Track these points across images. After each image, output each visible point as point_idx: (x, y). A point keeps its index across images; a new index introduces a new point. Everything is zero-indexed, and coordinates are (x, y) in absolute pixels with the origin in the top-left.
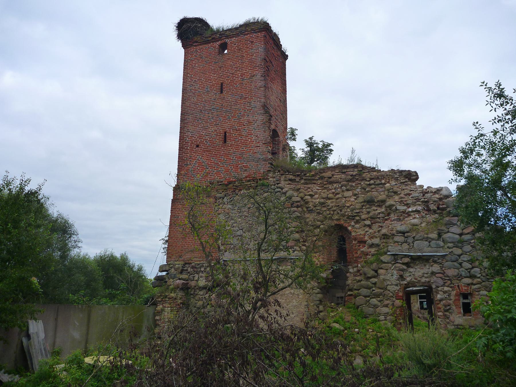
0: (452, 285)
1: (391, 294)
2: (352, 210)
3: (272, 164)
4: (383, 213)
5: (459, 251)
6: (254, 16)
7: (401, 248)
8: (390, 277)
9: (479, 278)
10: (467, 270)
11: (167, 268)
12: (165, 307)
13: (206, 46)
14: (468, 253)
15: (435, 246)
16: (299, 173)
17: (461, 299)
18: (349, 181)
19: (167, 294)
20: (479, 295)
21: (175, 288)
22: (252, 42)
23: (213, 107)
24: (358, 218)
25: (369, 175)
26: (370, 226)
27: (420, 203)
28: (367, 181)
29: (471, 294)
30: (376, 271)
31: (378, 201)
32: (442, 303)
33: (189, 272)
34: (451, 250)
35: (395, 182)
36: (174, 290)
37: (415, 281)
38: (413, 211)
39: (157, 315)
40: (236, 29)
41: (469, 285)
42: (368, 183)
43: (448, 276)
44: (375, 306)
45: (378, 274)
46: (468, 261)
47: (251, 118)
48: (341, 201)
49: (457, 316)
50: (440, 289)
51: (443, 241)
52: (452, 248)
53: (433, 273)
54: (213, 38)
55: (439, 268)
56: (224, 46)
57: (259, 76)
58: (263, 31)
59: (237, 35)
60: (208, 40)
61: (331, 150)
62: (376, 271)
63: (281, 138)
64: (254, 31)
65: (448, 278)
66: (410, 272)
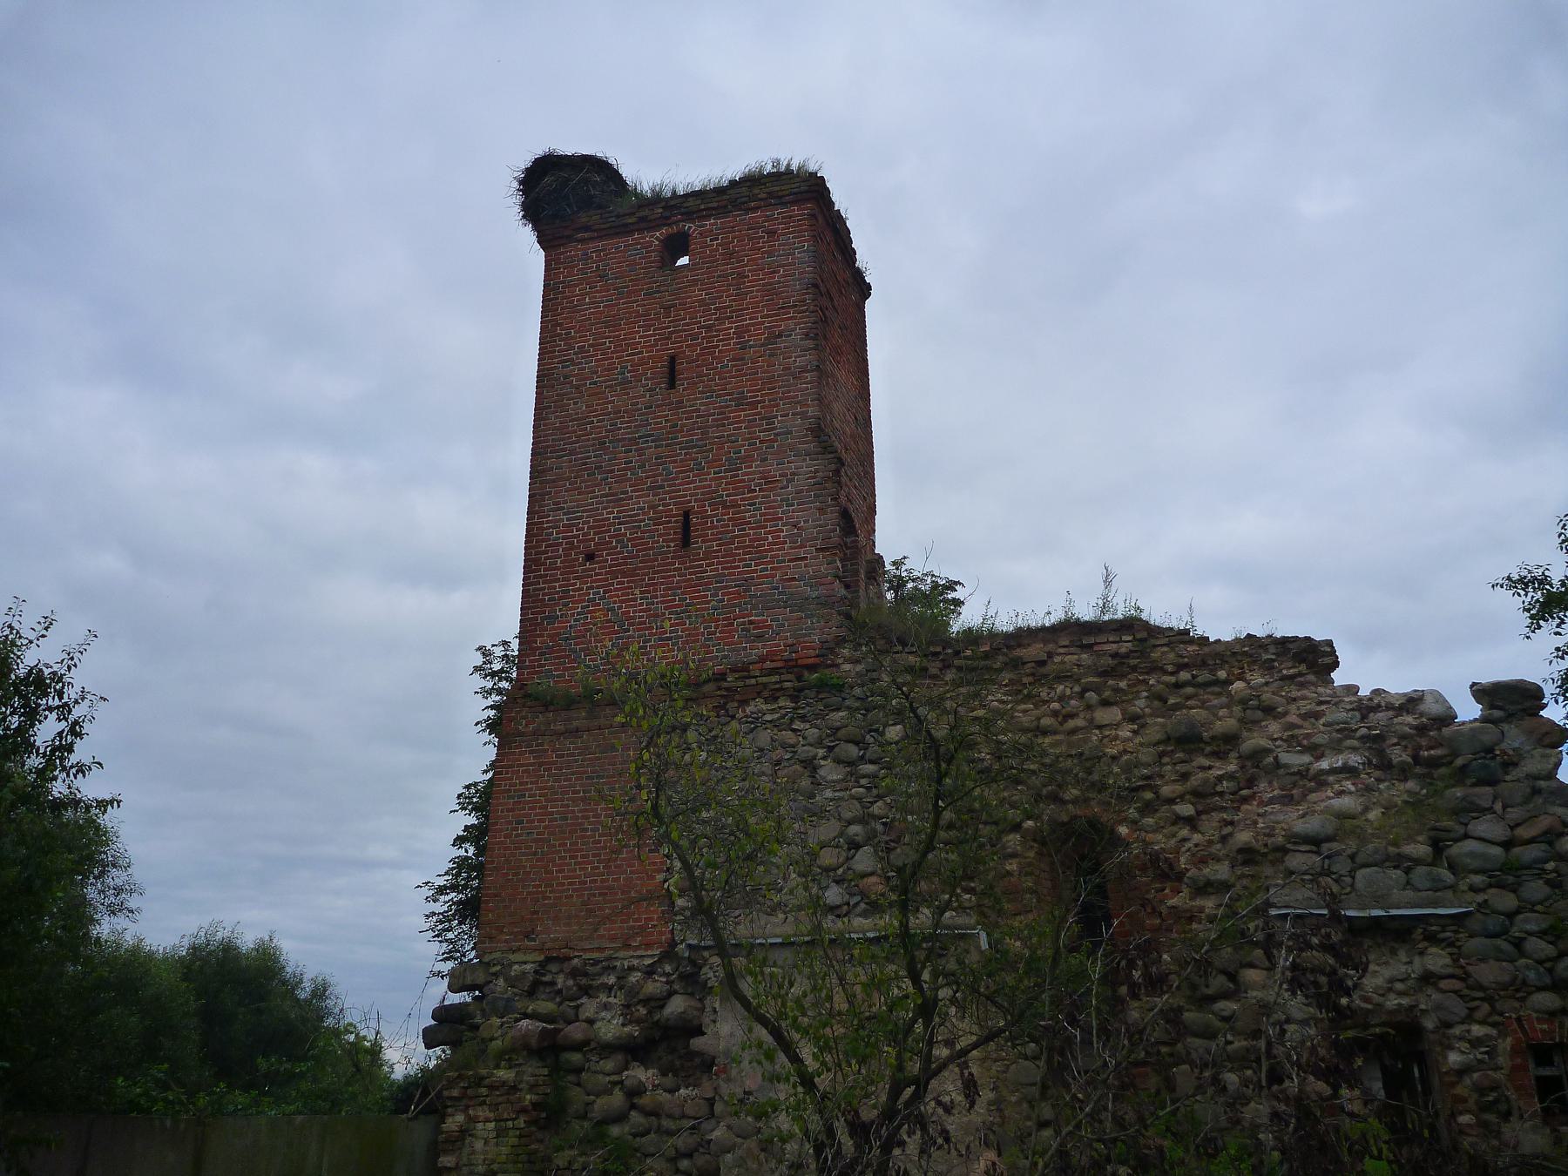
0: (1497, 1018)
2: (1128, 769)
3: (848, 616)
4: (1230, 777)
5: (1508, 901)
6: (775, 156)
11: (480, 978)
12: (475, 1120)
13: (621, 242)
14: (1539, 908)
15: (1428, 885)
16: (939, 649)
17: (1531, 1066)
18: (1105, 673)
19: (484, 1072)
21: (513, 1050)
22: (771, 233)
23: (643, 431)
24: (1149, 795)
25: (1172, 656)
26: (1191, 822)
27: (1355, 743)
28: (1166, 673)
30: (1232, 977)
31: (1213, 738)
32: (1467, 1081)
33: (559, 992)
34: (1480, 898)
35: (1263, 676)
36: (506, 1057)
37: (1364, 1005)
38: (1333, 771)
39: (446, 1152)
40: (719, 191)
42: (1172, 679)
43: (1481, 988)
46: (1542, 934)
47: (774, 469)
48: (1085, 741)
50: (1457, 1031)
51: (1452, 867)
53: (1428, 979)
54: (642, 219)
55: (1448, 961)
56: (678, 244)
57: (796, 337)
58: (808, 200)
59: (721, 211)
60: (626, 225)
61: (958, 603)
62: (1232, 977)
63: (862, 539)
64: (780, 200)
65: (1481, 994)
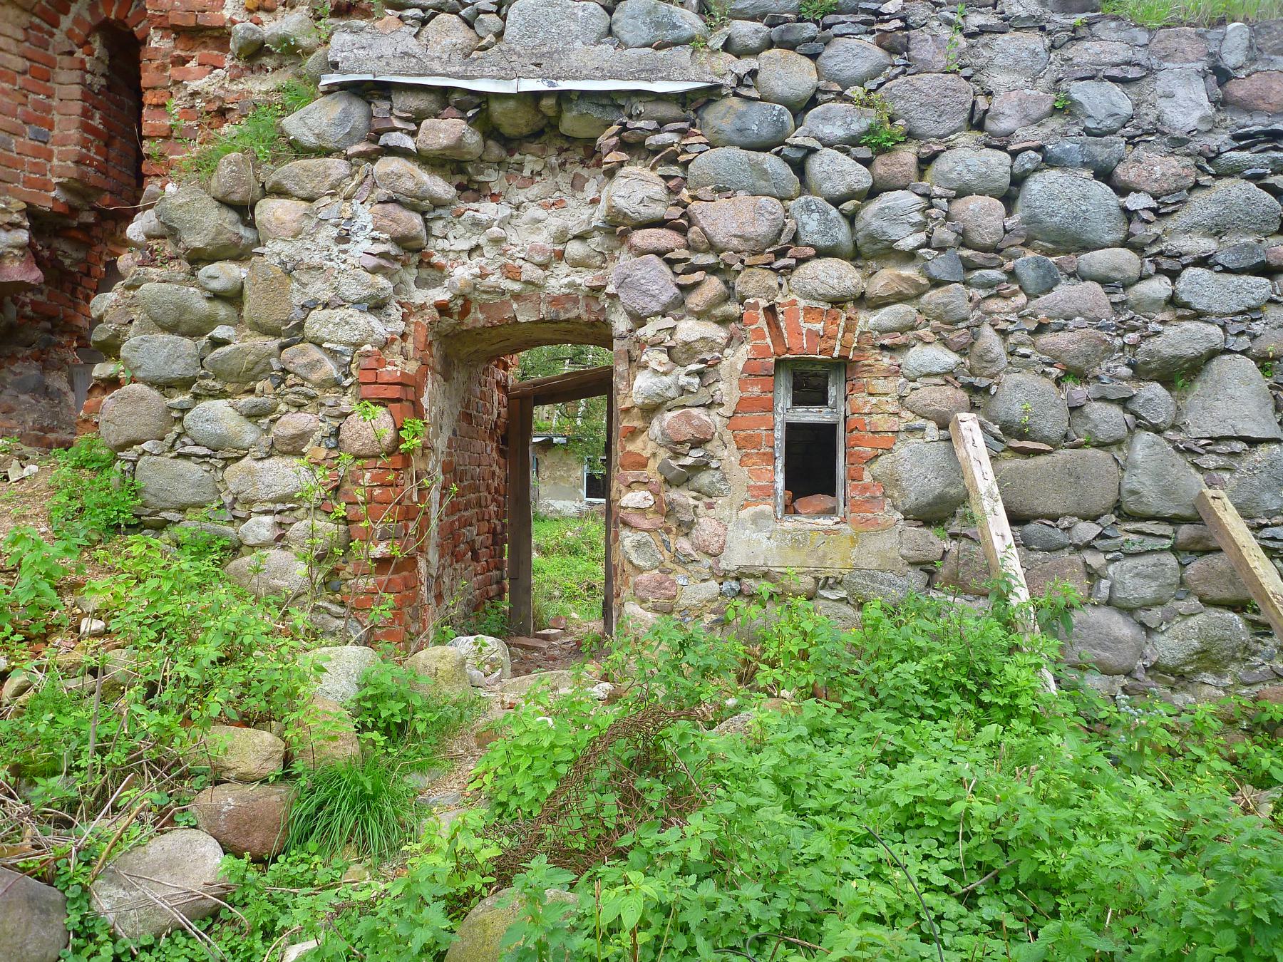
0: (733, 308)
1: (330, 368)
5: (789, 74)
7: (412, 45)
8: (329, 249)
9: (910, 256)
10: (836, 202)
14: (855, 92)
15: (645, 34)
17: (783, 399)
20: (896, 371)
29: (843, 366)
30: (244, 211)
32: (656, 427)
34: (743, 66)
41: (837, 302)
43: (712, 247)
44: (223, 453)
45: (251, 224)
46: (846, 145)
49: (746, 513)
50: (648, 331)
52: (754, 53)
53: (619, 227)
55: (658, 189)
62: (244, 211)
65: (710, 259)
66: (477, 225)
